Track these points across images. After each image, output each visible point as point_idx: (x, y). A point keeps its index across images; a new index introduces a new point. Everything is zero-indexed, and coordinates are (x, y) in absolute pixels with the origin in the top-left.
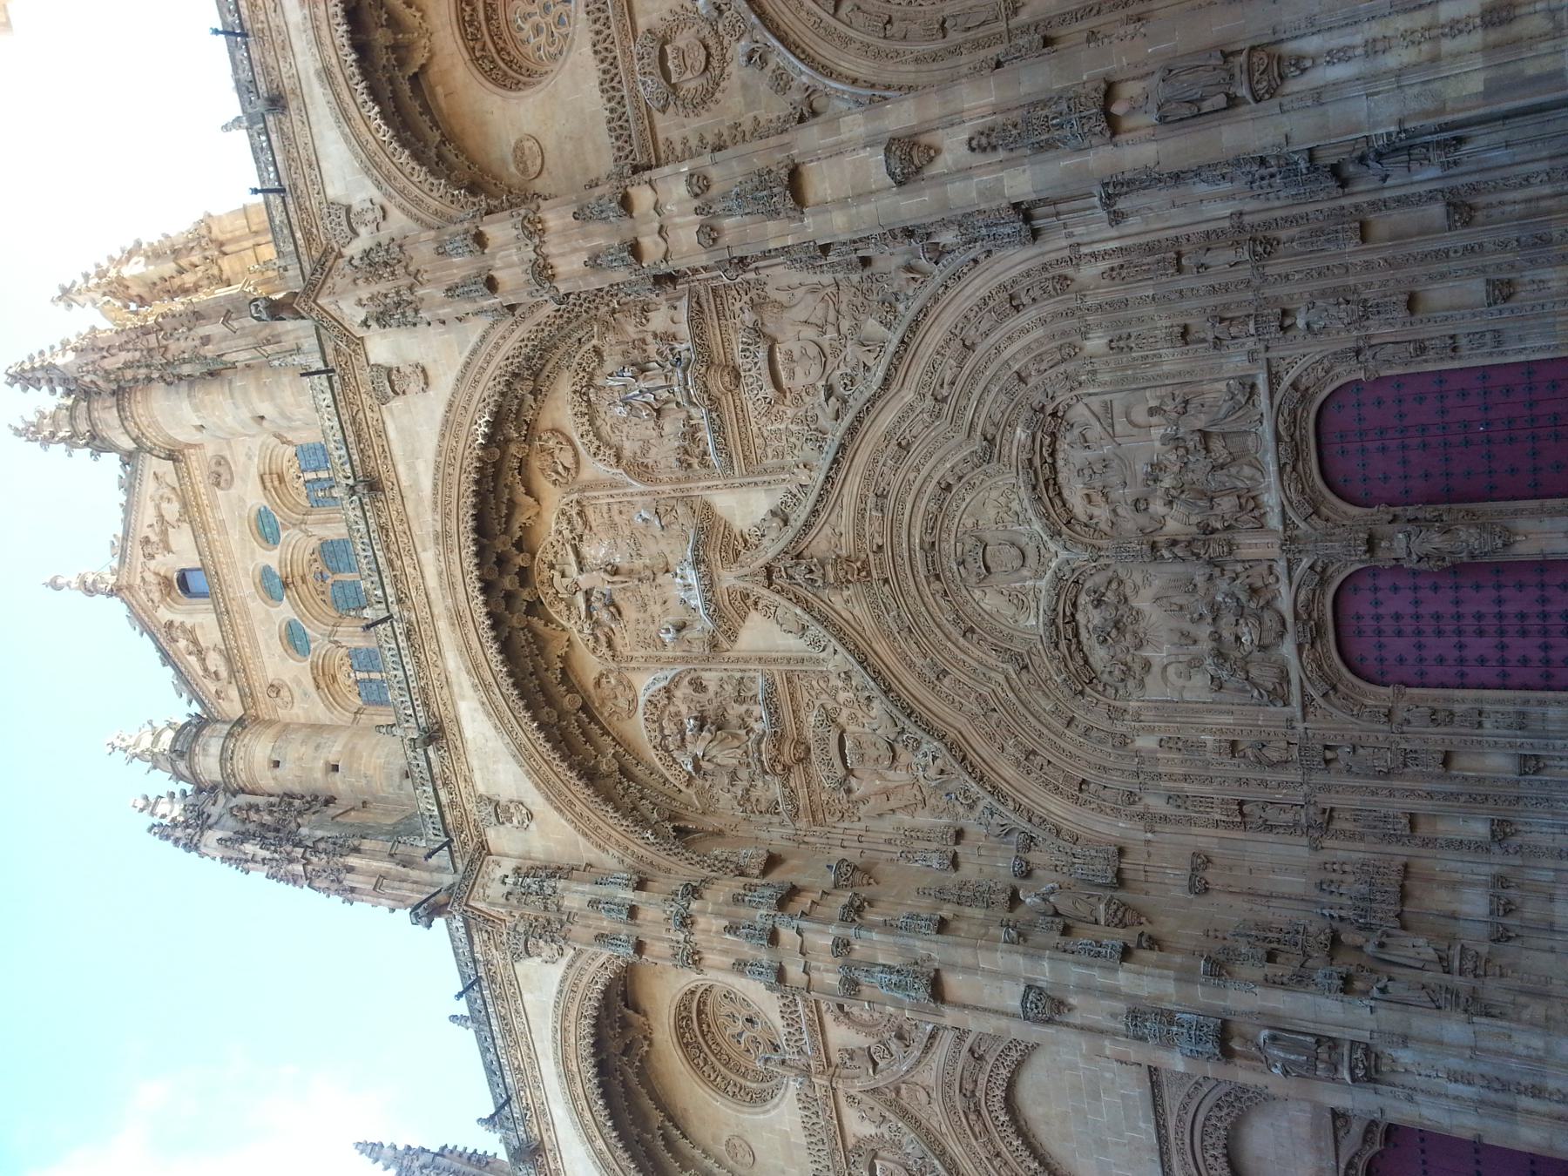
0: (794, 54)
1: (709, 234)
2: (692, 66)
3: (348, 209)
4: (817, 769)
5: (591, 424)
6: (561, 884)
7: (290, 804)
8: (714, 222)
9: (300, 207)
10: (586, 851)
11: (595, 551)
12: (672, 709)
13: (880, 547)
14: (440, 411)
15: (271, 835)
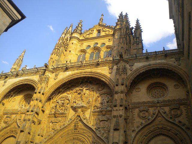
0: (140, 129)
1: (114, 117)
2: (143, 115)
3: (133, 66)
4: (54, 119)
5: (103, 94)
6: (45, 83)
7: (67, 45)
8: (116, 117)
9: (134, 59)
10: (49, 86)
11: (88, 92)
12: (66, 100)
13: (79, 132)
14: (106, 74)
15: (63, 43)
